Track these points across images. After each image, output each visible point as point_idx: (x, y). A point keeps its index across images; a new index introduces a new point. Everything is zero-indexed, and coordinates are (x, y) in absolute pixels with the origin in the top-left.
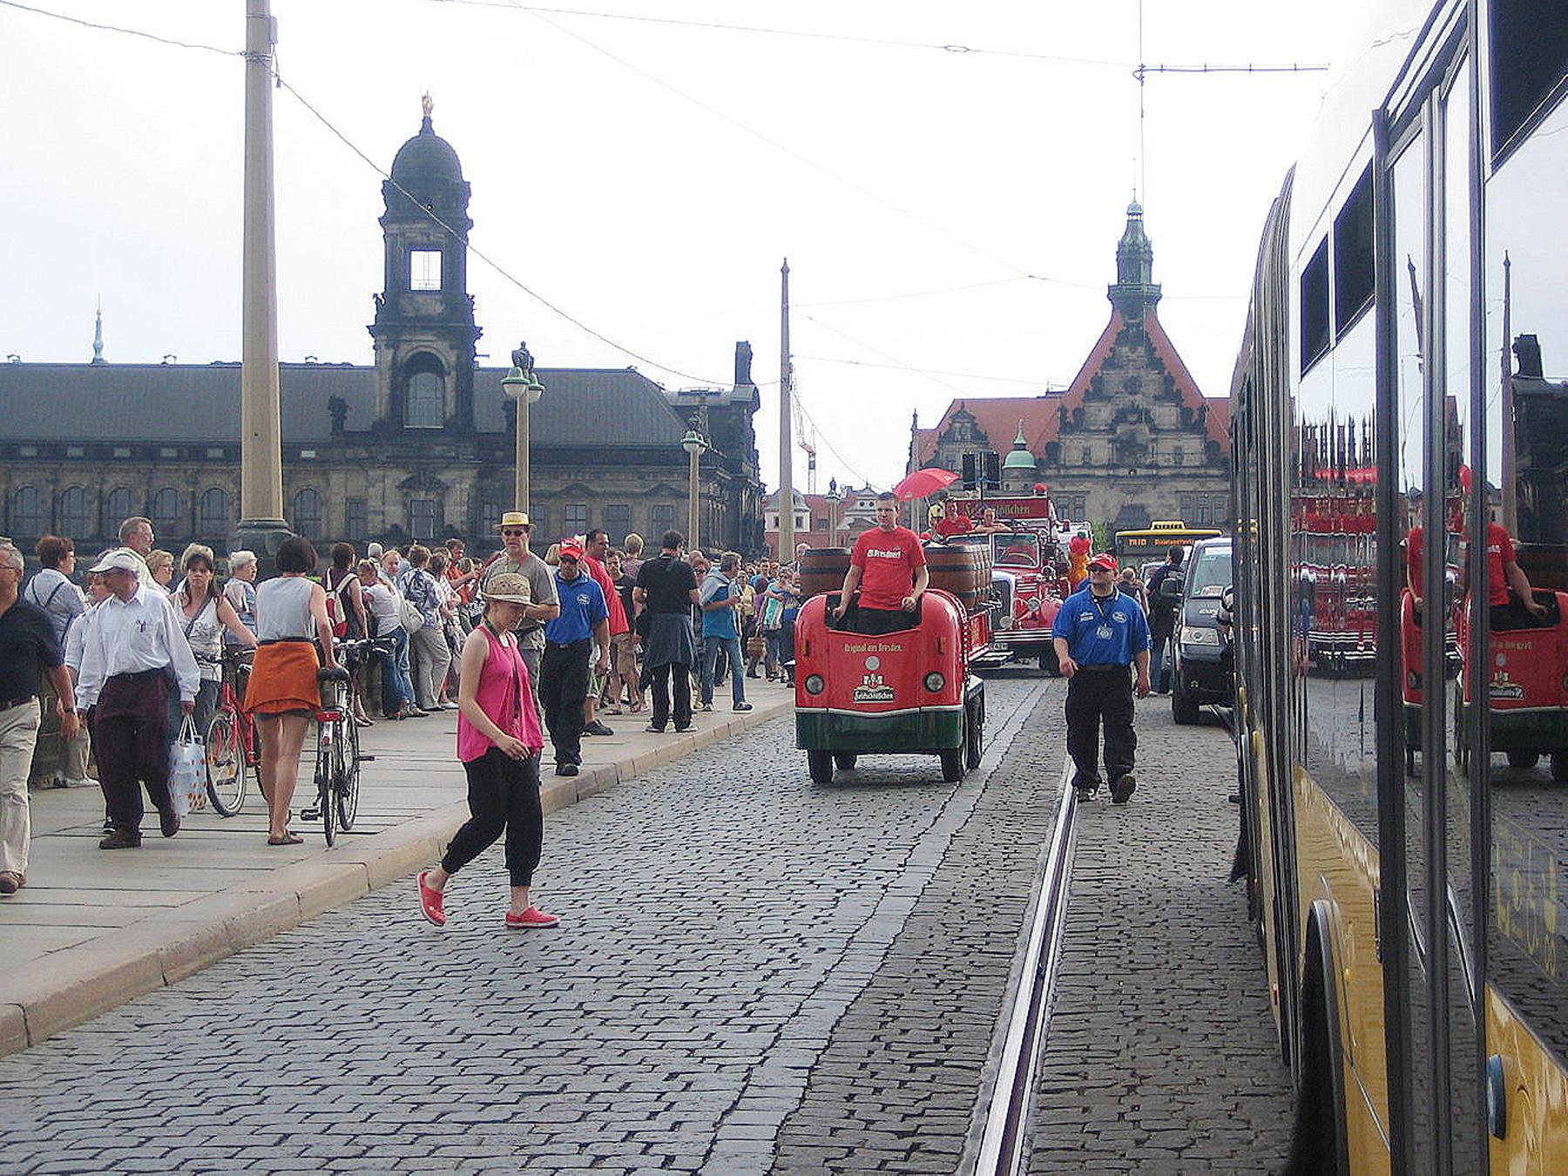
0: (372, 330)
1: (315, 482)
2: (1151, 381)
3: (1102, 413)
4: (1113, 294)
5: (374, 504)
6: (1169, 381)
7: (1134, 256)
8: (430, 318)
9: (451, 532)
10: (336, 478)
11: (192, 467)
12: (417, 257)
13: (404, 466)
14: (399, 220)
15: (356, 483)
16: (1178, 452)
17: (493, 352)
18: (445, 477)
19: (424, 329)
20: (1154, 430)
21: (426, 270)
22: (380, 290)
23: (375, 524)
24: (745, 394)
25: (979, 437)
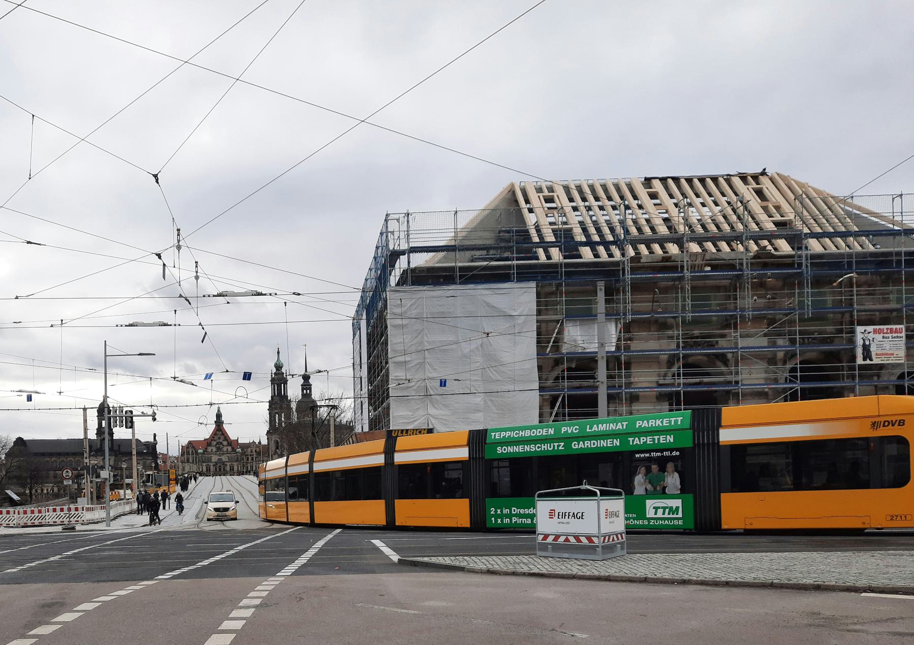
3: (215, 443)
7: (219, 416)
25: (193, 447)
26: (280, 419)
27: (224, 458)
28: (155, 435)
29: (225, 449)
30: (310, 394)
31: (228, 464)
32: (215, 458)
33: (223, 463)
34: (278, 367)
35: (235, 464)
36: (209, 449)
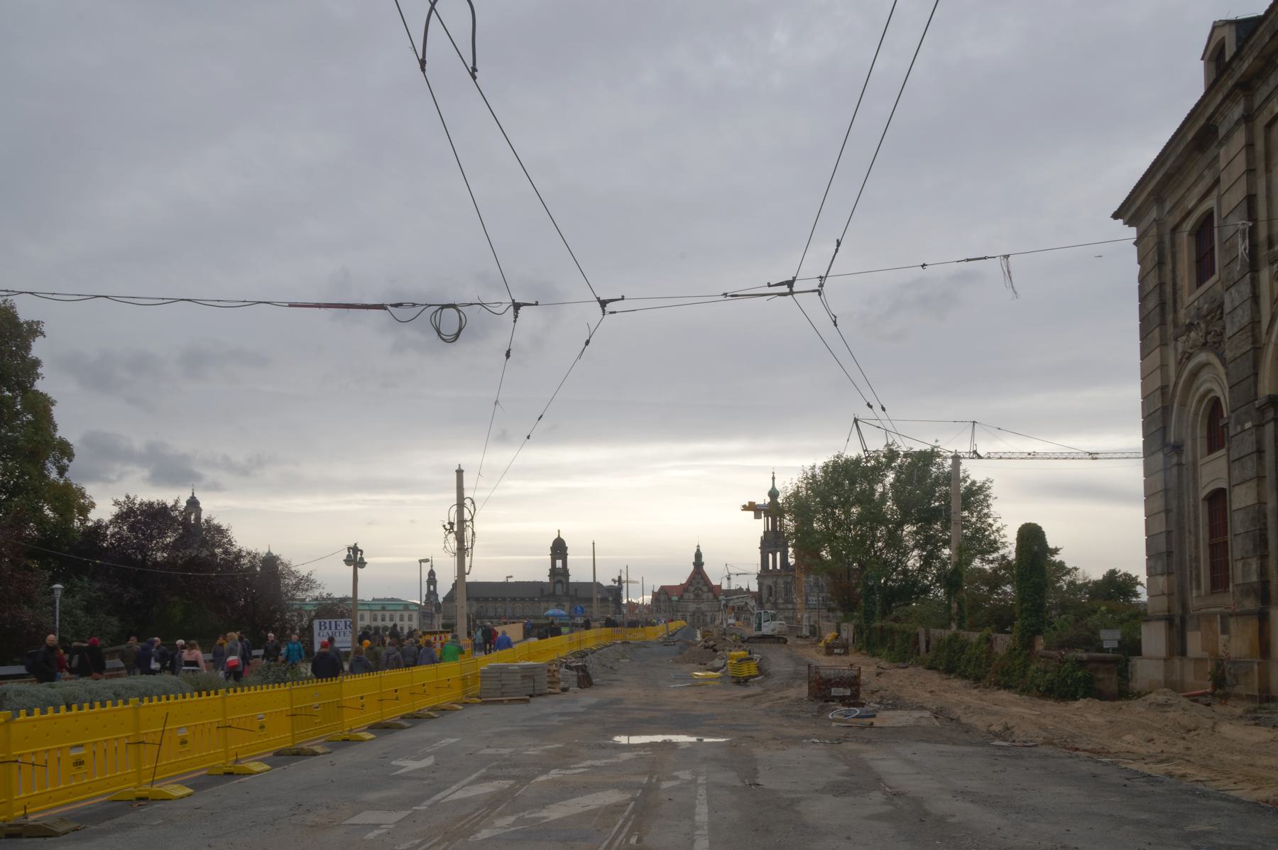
2: (702, 582)
3: (692, 589)
7: (698, 555)
17: (571, 580)
21: (559, 563)
27: (704, 607)
29: (705, 596)
32: (692, 607)
33: (703, 613)
36: (686, 596)
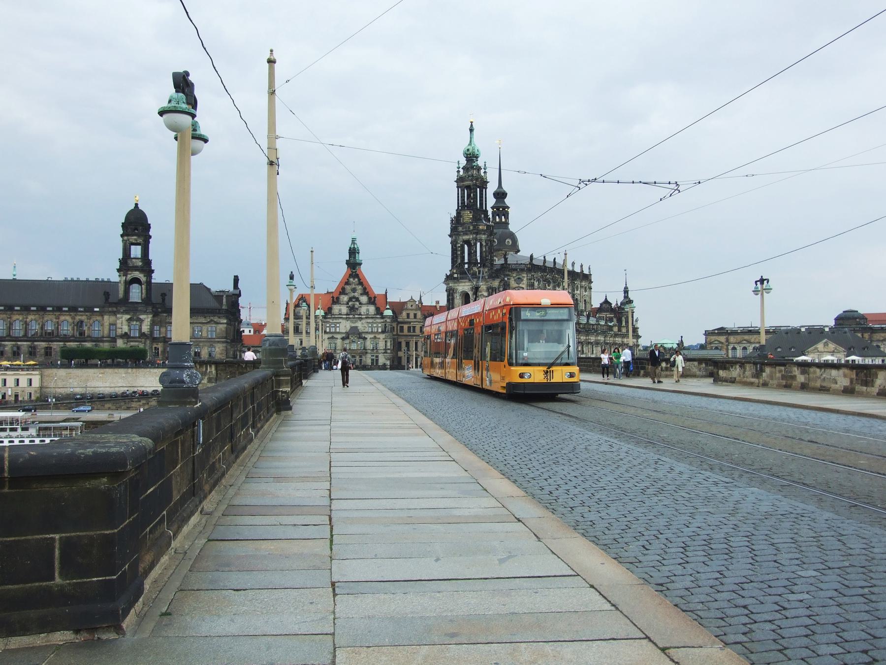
0: (119, 270)
1: (99, 318)
4: (348, 263)
5: (119, 325)
6: (365, 289)
7: (353, 252)
8: (137, 267)
9: (142, 335)
10: (106, 317)
11: (57, 313)
12: (133, 247)
13: (127, 313)
14: (127, 235)
15: (112, 318)
16: (368, 310)
18: (142, 317)
19: (136, 270)
20: (360, 304)
22: (121, 257)
23: (119, 332)
24: (237, 292)
26: (472, 254)
27: (361, 325)
28: (236, 280)
29: (363, 310)
30: (506, 224)
31: (369, 336)
32: (344, 326)
33: (360, 336)
34: (471, 157)
35: (382, 336)
36: (336, 309)
